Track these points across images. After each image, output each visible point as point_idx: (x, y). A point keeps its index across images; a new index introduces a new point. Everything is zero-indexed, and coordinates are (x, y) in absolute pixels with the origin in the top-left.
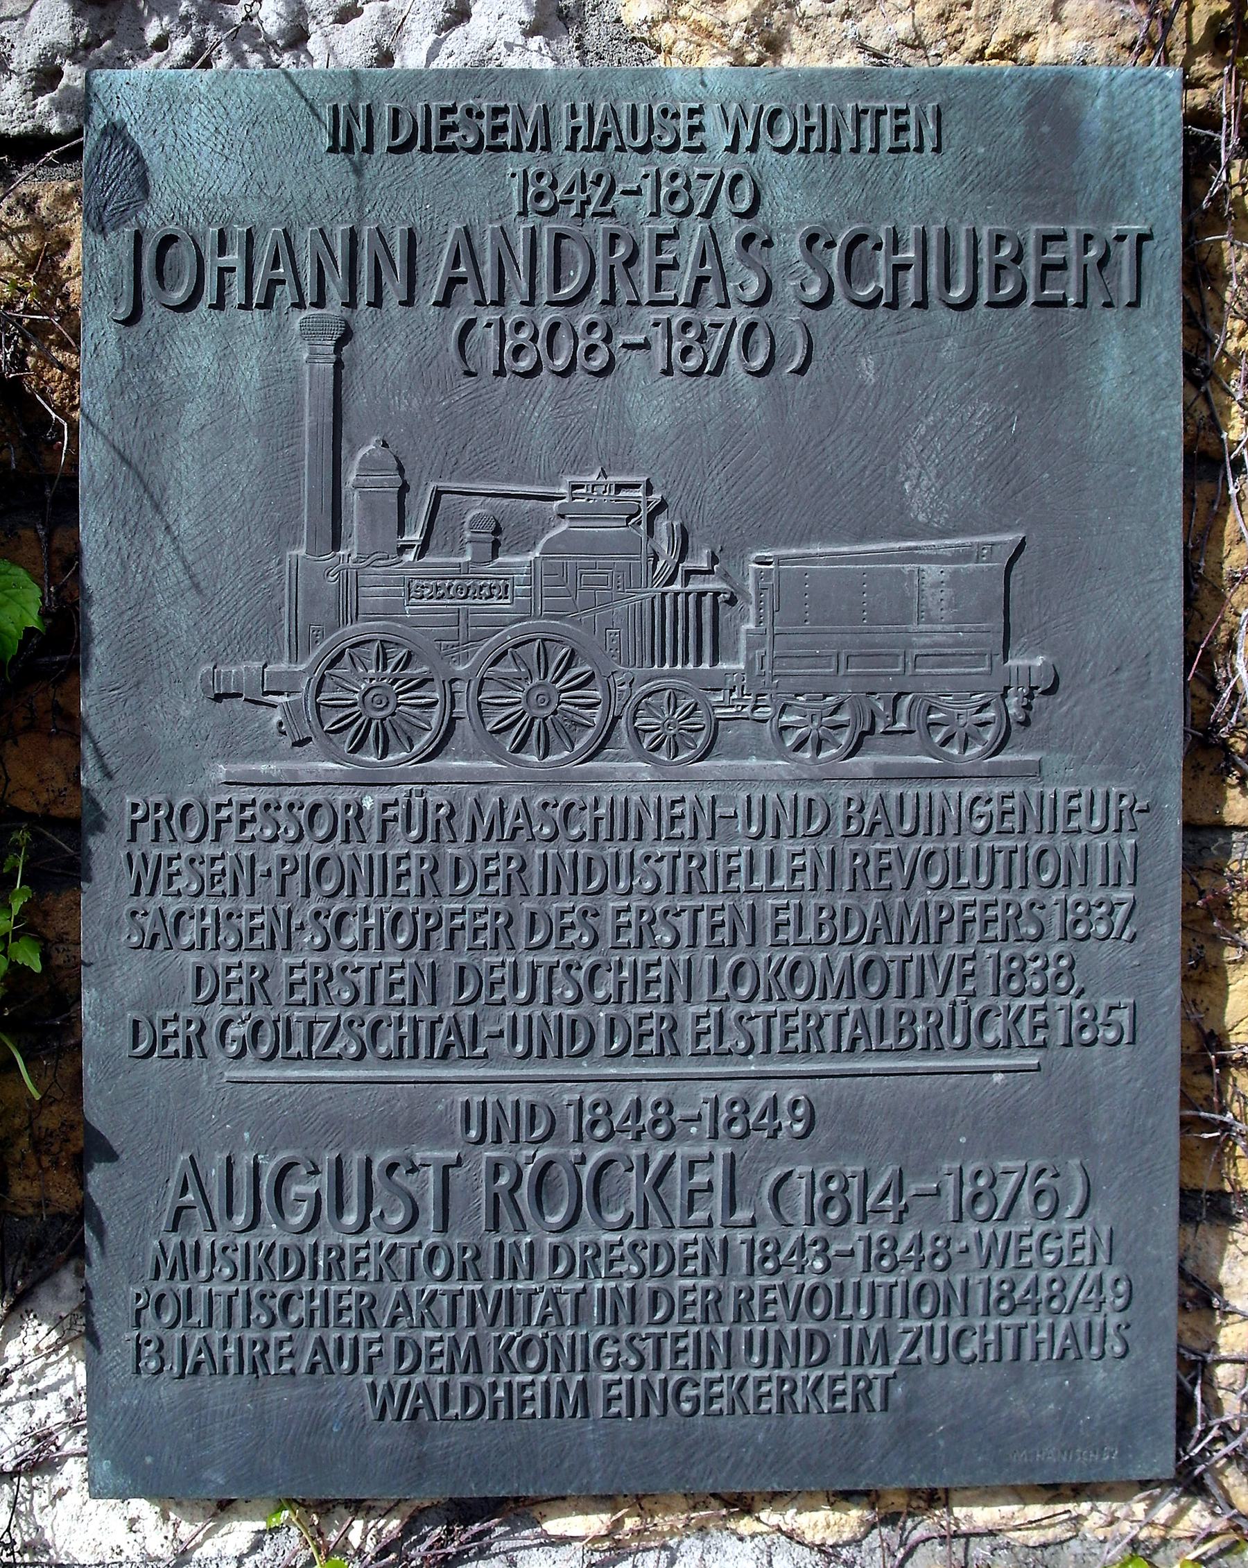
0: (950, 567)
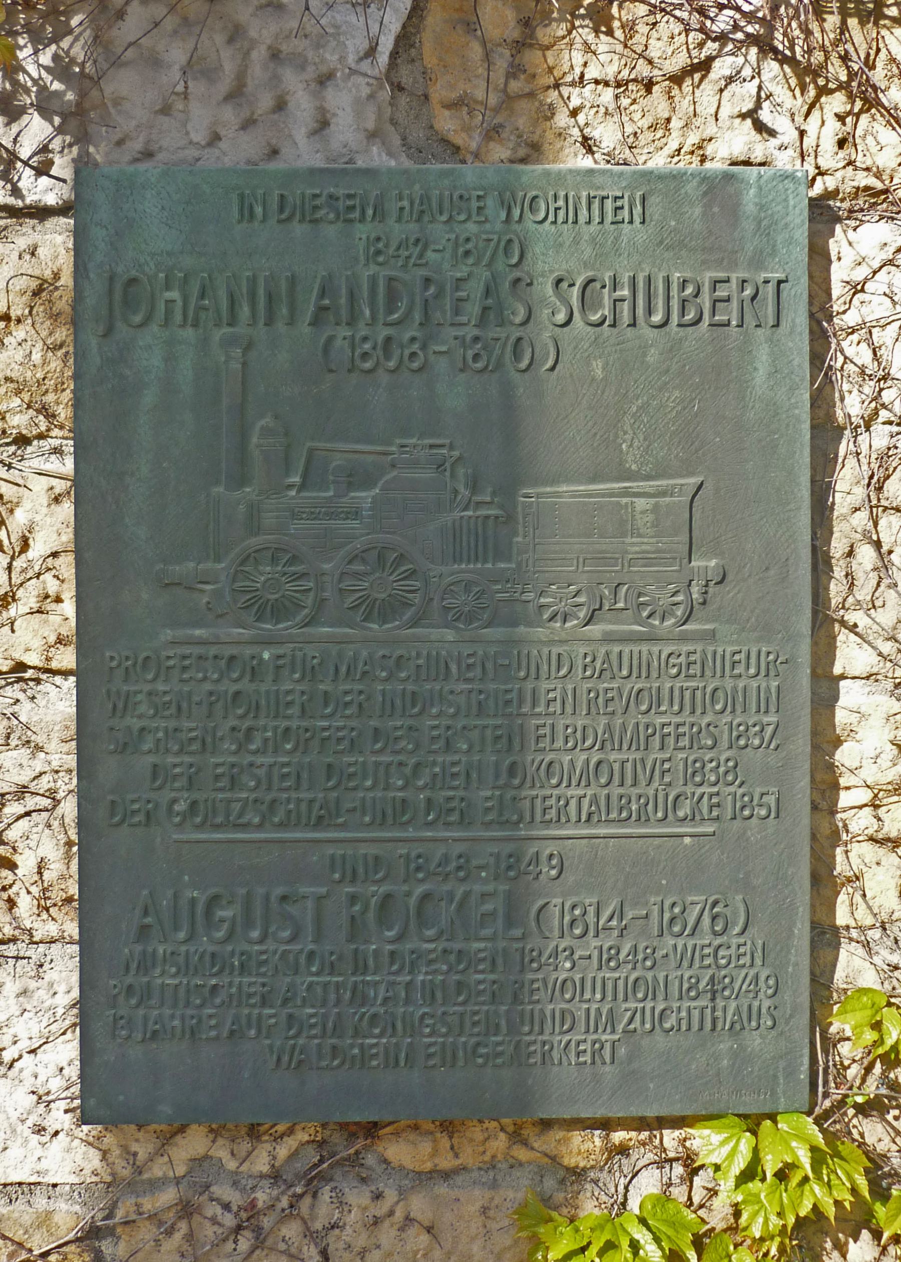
0: (653, 501)
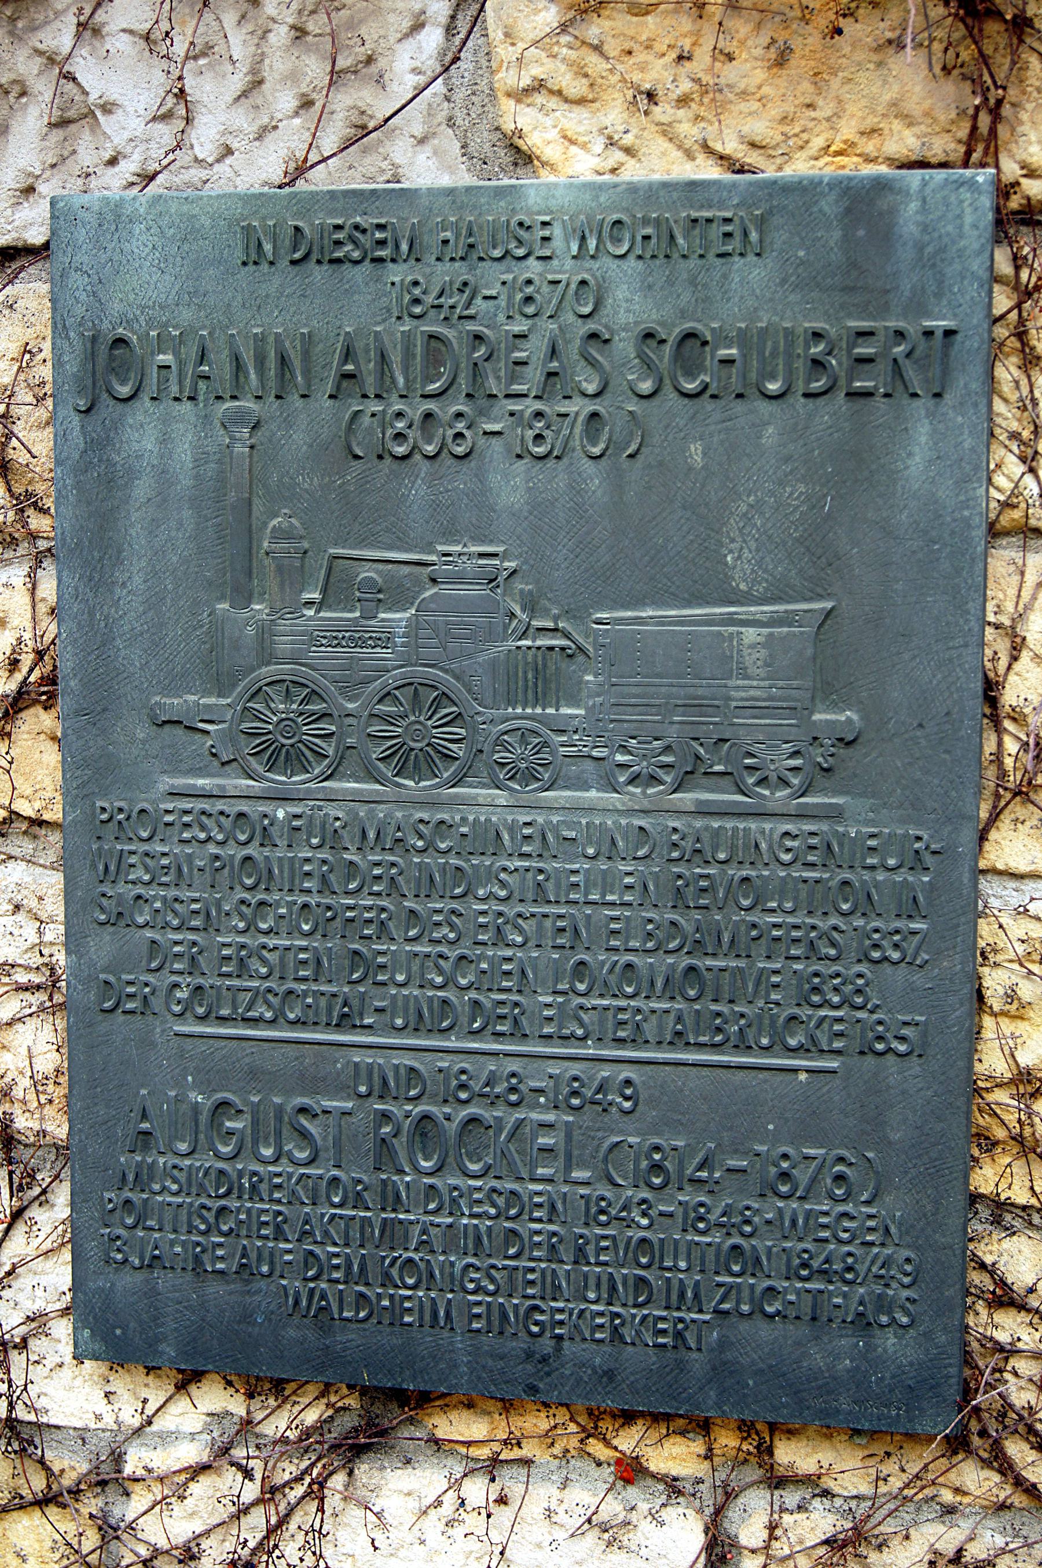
0: (765, 631)
